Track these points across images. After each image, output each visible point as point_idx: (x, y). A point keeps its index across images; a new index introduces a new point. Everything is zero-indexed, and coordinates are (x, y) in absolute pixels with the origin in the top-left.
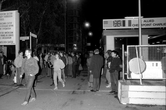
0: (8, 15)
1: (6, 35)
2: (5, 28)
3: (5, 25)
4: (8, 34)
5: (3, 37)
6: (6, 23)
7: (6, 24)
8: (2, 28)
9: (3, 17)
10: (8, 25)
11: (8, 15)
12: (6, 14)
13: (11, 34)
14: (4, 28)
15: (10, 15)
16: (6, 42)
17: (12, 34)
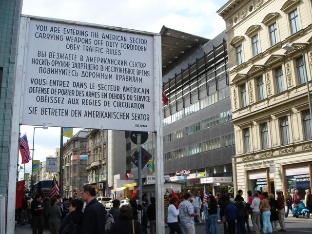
0: (132, 44)
1: (126, 96)
2: (125, 75)
3: (125, 67)
4: (133, 94)
5: (117, 100)
6: (128, 63)
7: (128, 67)
8: (114, 74)
9: (119, 45)
10: (133, 68)
11: (132, 44)
12: (128, 39)
13: (143, 95)
14: (122, 74)
15: (141, 45)
16: (128, 116)
17: (146, 95)
